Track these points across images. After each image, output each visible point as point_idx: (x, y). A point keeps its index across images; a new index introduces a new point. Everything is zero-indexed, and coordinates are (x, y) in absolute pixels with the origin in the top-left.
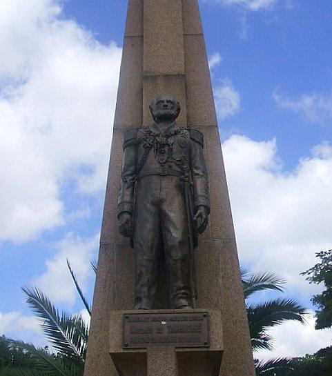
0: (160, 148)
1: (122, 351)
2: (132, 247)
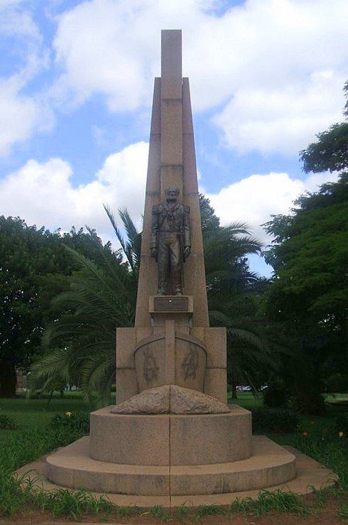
0: (170, 218)
2: (157, 261)
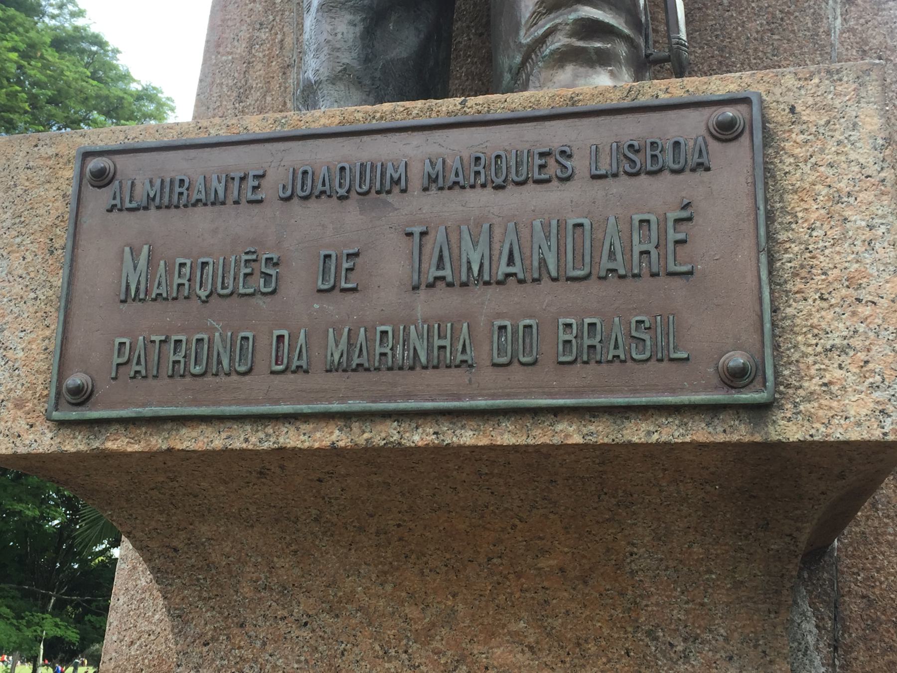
1: (43, 441)
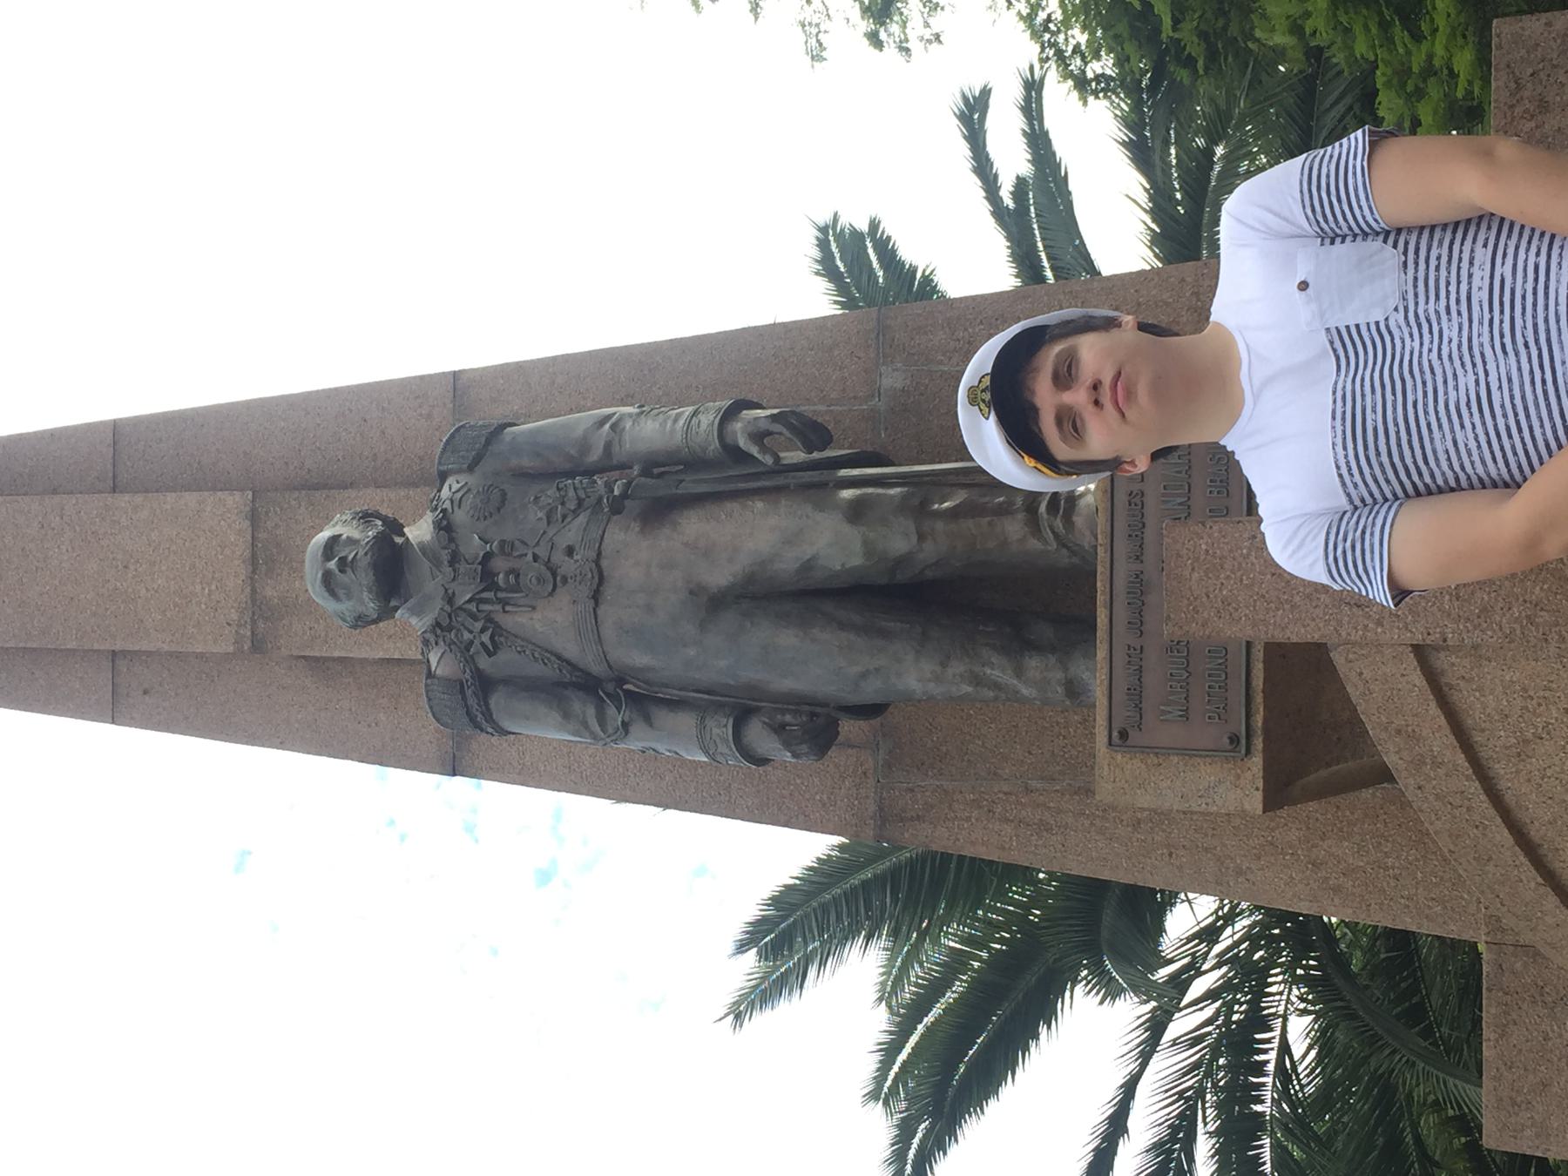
1: (1257, 762)
